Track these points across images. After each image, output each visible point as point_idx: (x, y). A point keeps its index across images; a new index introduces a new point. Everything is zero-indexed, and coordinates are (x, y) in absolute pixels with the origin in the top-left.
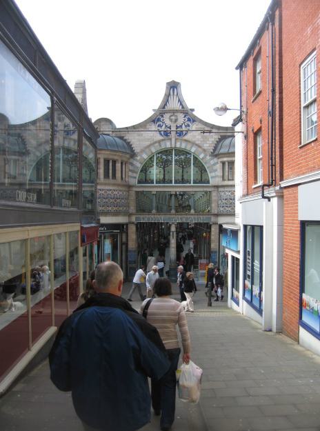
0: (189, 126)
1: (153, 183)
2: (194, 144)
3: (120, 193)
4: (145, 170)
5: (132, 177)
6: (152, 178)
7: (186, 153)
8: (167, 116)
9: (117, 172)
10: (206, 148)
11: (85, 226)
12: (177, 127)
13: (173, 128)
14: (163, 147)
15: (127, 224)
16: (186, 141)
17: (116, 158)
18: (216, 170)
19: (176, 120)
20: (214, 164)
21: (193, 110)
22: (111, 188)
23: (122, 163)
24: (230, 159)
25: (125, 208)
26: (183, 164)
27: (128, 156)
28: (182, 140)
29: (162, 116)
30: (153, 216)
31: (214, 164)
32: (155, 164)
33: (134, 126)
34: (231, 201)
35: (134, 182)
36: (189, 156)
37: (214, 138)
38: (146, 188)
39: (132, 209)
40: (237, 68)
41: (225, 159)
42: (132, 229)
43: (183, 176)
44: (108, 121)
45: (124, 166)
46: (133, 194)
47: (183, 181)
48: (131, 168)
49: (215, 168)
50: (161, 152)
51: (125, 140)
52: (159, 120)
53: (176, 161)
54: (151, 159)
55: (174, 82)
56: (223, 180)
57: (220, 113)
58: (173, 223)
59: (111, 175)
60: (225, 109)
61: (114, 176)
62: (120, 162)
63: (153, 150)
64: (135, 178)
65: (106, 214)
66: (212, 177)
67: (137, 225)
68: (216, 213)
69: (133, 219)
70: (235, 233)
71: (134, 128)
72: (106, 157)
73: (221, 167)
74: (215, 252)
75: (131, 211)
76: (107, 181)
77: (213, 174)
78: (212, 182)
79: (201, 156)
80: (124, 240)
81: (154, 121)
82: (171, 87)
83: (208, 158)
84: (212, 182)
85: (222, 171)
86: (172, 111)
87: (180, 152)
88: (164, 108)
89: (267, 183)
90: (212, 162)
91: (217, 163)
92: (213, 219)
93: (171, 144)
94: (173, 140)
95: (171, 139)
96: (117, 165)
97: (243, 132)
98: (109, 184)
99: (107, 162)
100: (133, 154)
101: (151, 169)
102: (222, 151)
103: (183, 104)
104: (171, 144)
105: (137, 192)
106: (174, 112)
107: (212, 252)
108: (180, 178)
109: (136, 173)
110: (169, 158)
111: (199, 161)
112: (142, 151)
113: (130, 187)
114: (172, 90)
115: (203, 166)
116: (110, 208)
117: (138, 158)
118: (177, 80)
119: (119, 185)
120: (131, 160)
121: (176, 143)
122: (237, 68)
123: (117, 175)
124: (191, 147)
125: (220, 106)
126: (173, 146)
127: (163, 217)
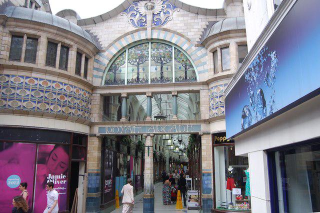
2: (175, 32)
5: (96, 76)
14: (137, 39)
16: (166, 30)
17: (68, 42)
18: (205, 63)
19: (152, 8)
20: (202, 57)
23: (79, 54)
24: (222, 43)
25: (80, 113)
28: (159, 29)
29: (136, 5)
30: (121, 126)
31: (202, 57)
32: (126, 61)
35: (97, 82)
36: (169, 49)
37: (200, 23)
39: (95, 117)
41: (216, 44)
48: (96, 65)
49: (202, 60)
51: (91, 34)
54: (122, 52)
56: (215, 71)
58: (148, 135)
59: (58, 62)
61: (64, 64)
63: (124, 43)
66: (200, 72)
68: (207, 117)
71: (103, 18)
73: (212, 58)
74: (209, 175)
75: (93, 120)
77: (201, 68)
78: (200, 78)
81: (125, 10)
83: (194, 48)
84: (200, 78)
85: (212, 63)
91: (206, 54)
92: (203, 128)
94: (149, 29)
95: (146, 29)
98: (52, 73)
99: (52, 44)
100: (98, 51)
102: (210, 35)
104: (146, 35)
105: (101, 95)
107: (204, 175)
108: (159, 76)
110: (145, 53)
112: (111, 45)
113: (93, 88)
116: (52, 107)
117: (105, 54)
120: (97, 57)
121: (152, 34)
123: (69, 66)
124: (172, 38)
126: (149, 37)
127: (134, 126)
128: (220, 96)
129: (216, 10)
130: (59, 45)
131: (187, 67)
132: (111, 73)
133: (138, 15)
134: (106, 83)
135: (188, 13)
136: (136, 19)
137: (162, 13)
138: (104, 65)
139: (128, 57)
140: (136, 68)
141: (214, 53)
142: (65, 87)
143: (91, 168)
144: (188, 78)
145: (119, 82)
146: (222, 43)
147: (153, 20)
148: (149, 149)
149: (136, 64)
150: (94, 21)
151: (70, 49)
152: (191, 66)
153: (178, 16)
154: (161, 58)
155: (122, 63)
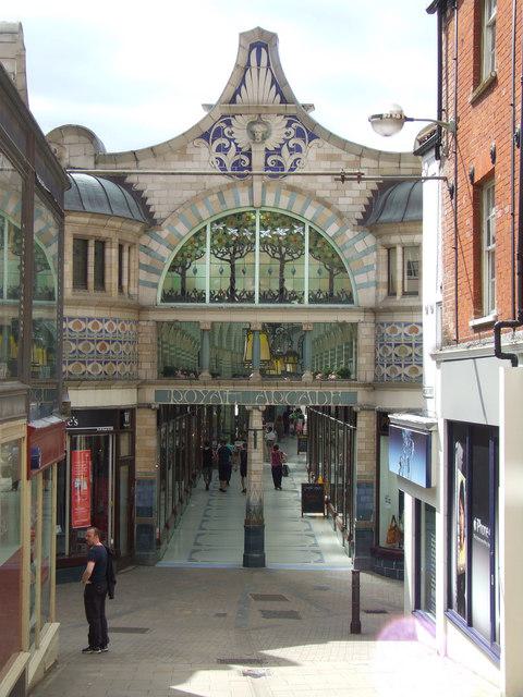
0: (299, 149)
1: (203, 300)
2: (312, 197)
3: (117, 327)
4: (180, 266)
5: (146, 284)
6: (199, 288)
7: (289, 221)
8: (240, 123)
9: (107, 270)
10: (343, 209)
11: (39, 424)
12: (268, 153)
13: (258, 159)
15: (132, 411)
16: (292, 189)
17: (104, 233)
20: (365, 253)
21: (311, 107)
22: (92, 313)
23: (121, 248)
24: (406, 239)
25: (127, 368)
26: (283, 251)
27: (137, 228)
29: (229, 124)
30: (201, 389)
31: (365, 253)
32: (208, 250)
33: (152, 149)
34: (410, 350)
38: (184, 314)
39: (148, 369)
40: (430, 10)
42: (146, 423)
43: (282, 281)
44: (86, 135)
45: (125, 255)
46: (147, 327)
47: (282, 296)
48: (145, 259)
50: (224, 219)
51: (129, 187)
52: (219, 133)
53: (264, 242)
54: (198, 236)
55: (260, 31)
57: (388, 128)
59: (91, 279)
60: (400, 120)
62: (116, 244)
64: (155, 286)
65: (81, 381)
66: (361, 286)
67: (158, 412)
69: (150, 395)
70: (423, 441)
71: (152, 151)
72: (77, 230)
75: (142, 374)
76: (81, 295)
77: (360, 279)
79: (332, 230)
80: (124, 451)
81: (205, 136)
82: (252, 46)
83: (349, 234)
86: (259, 107)
87: (274, 219)
88: (233, 100)
89: (507, 318)
90: (360, 247)
92: (362, 397)
93: (251, 197)
96: (107, 251)
97: (445, 179)
98: (87, 304)
99: (81, 244)
101: (197, 264)
103: (284, 90)
104: (251, 197)
106: (259, 115)
108: (275, 287)
109: (158, 273)
110: (247, 233)
111: (326, 243)
113: (141, 309)
114: (254, 52)
115: (335, 255)
116: (89, 368)
117: (165, 233)
118: (269, 27)
119: (112, 306)
120: (145, 240)
122: (430, 10)
123: (107, 281)
124: (305, 207)
125: (385, 111)
128: (396, 345)
129: (400, 154)
130: (91, 243)
132: (175, 274)
133: (233, 149)
134: (167, 297)
135: (337, 151)
136: (230, 158)
137: (285, 149)
138: (163, 259)
139: (212, 241)
140: (227, 267)
141: (389, 250)
142: (106, 326)
143: (142, 470)
144: (335, 294)
145: (193, 296)
146: (406, 239)
147: (266, 164)
148: (255, 435)
149: (228, 257)
150: (135, 155)
151: (108, 244)
152: (342, 269)
153: (319, 157)
154: (280, 249)
155: (198, 253)
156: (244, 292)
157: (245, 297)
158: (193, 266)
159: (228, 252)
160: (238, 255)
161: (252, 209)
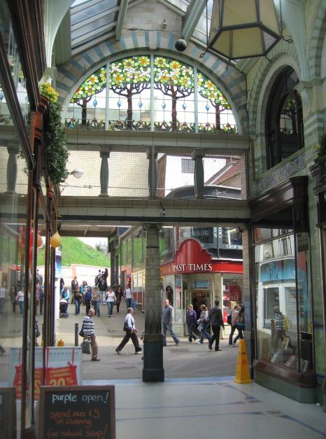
43: (174, 114)
131: (221, 108)
145: (93, 125)
149: (125, 92)
154: (172, 87)
156: (141, 123)
157: (141, 127)
158: (93, 99)
159: (125, 88)
160: (134, 91)
161: (148, 53)
